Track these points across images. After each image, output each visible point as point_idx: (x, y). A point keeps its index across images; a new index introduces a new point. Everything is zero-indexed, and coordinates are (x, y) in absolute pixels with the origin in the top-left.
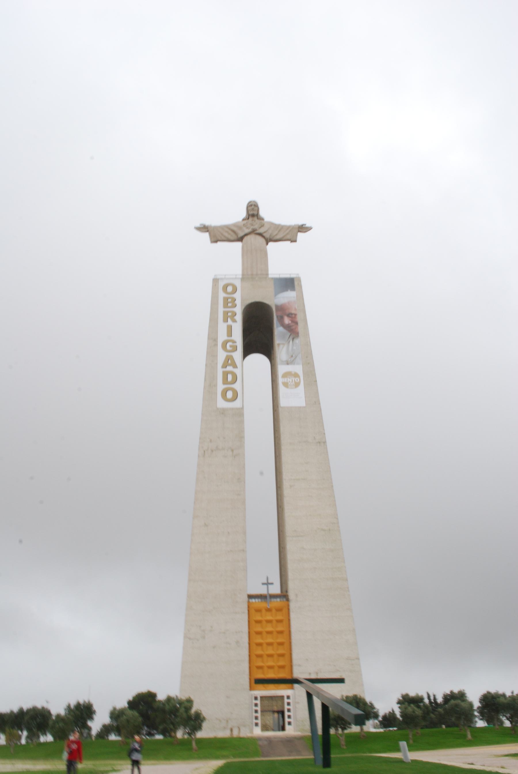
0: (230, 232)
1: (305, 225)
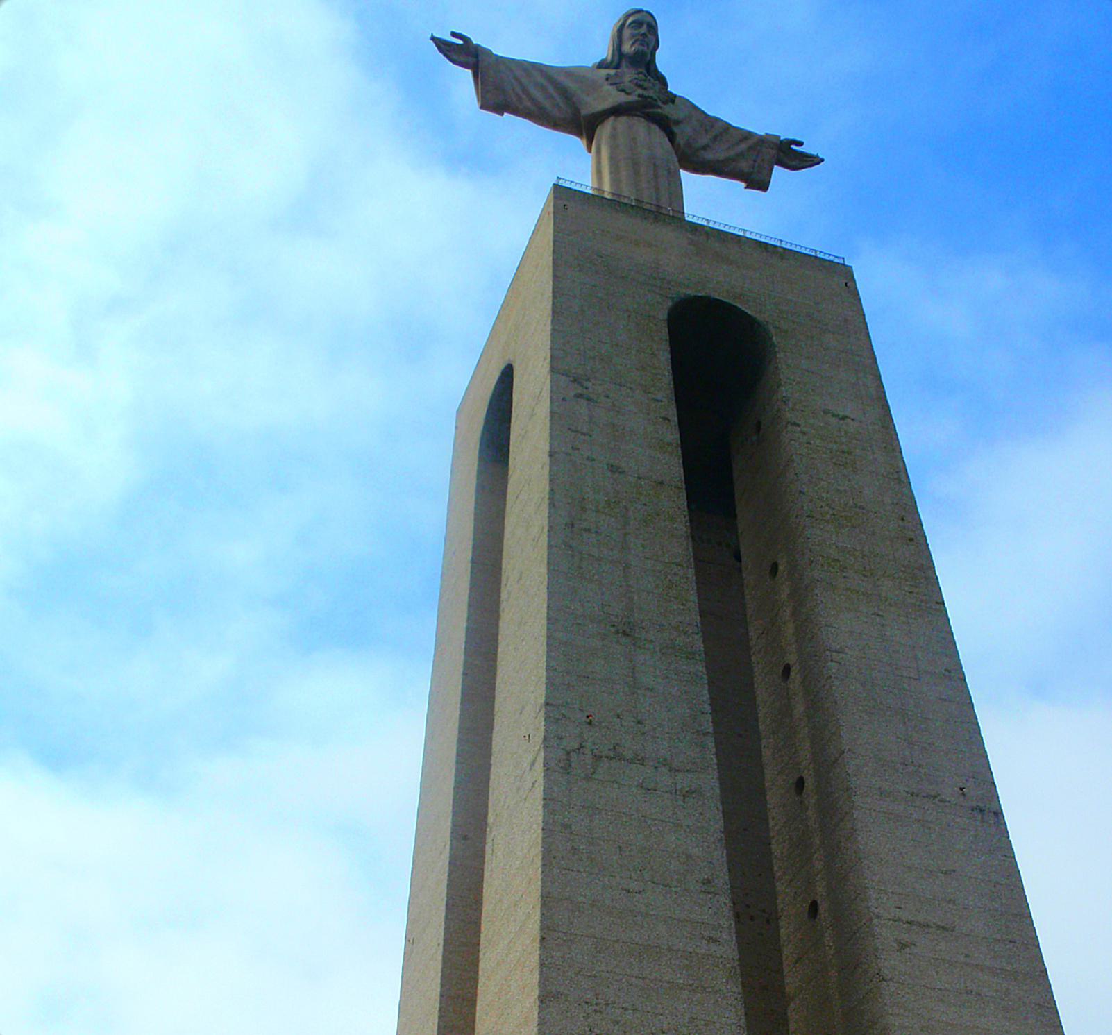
0: (551, 89)
1: (800, 144)
